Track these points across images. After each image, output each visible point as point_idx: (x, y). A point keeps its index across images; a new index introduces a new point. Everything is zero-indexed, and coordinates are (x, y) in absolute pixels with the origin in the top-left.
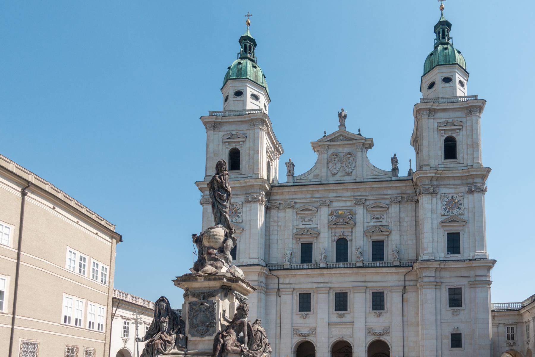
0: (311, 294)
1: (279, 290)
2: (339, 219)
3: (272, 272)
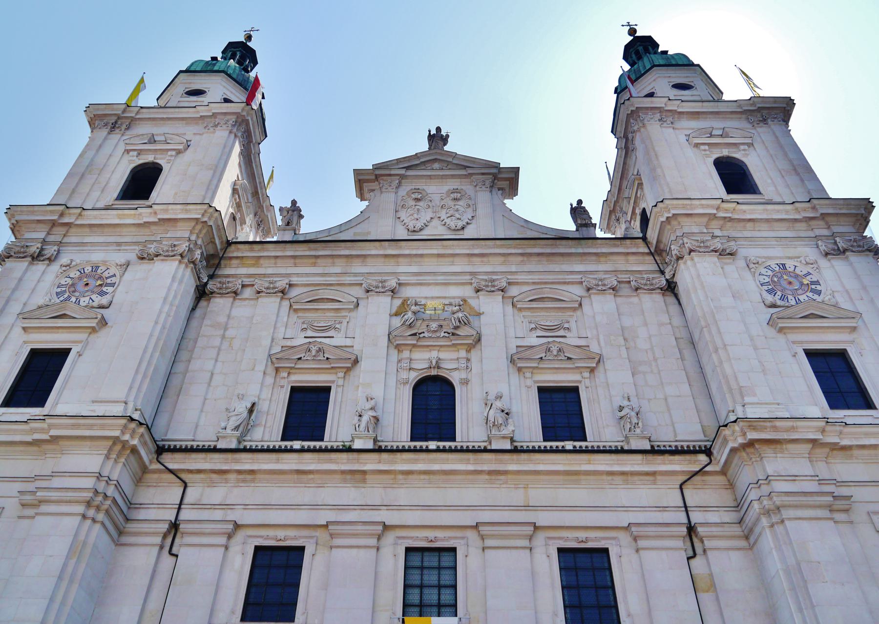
1: (174, 526)
2: (426, 323)
3: (167, 458)
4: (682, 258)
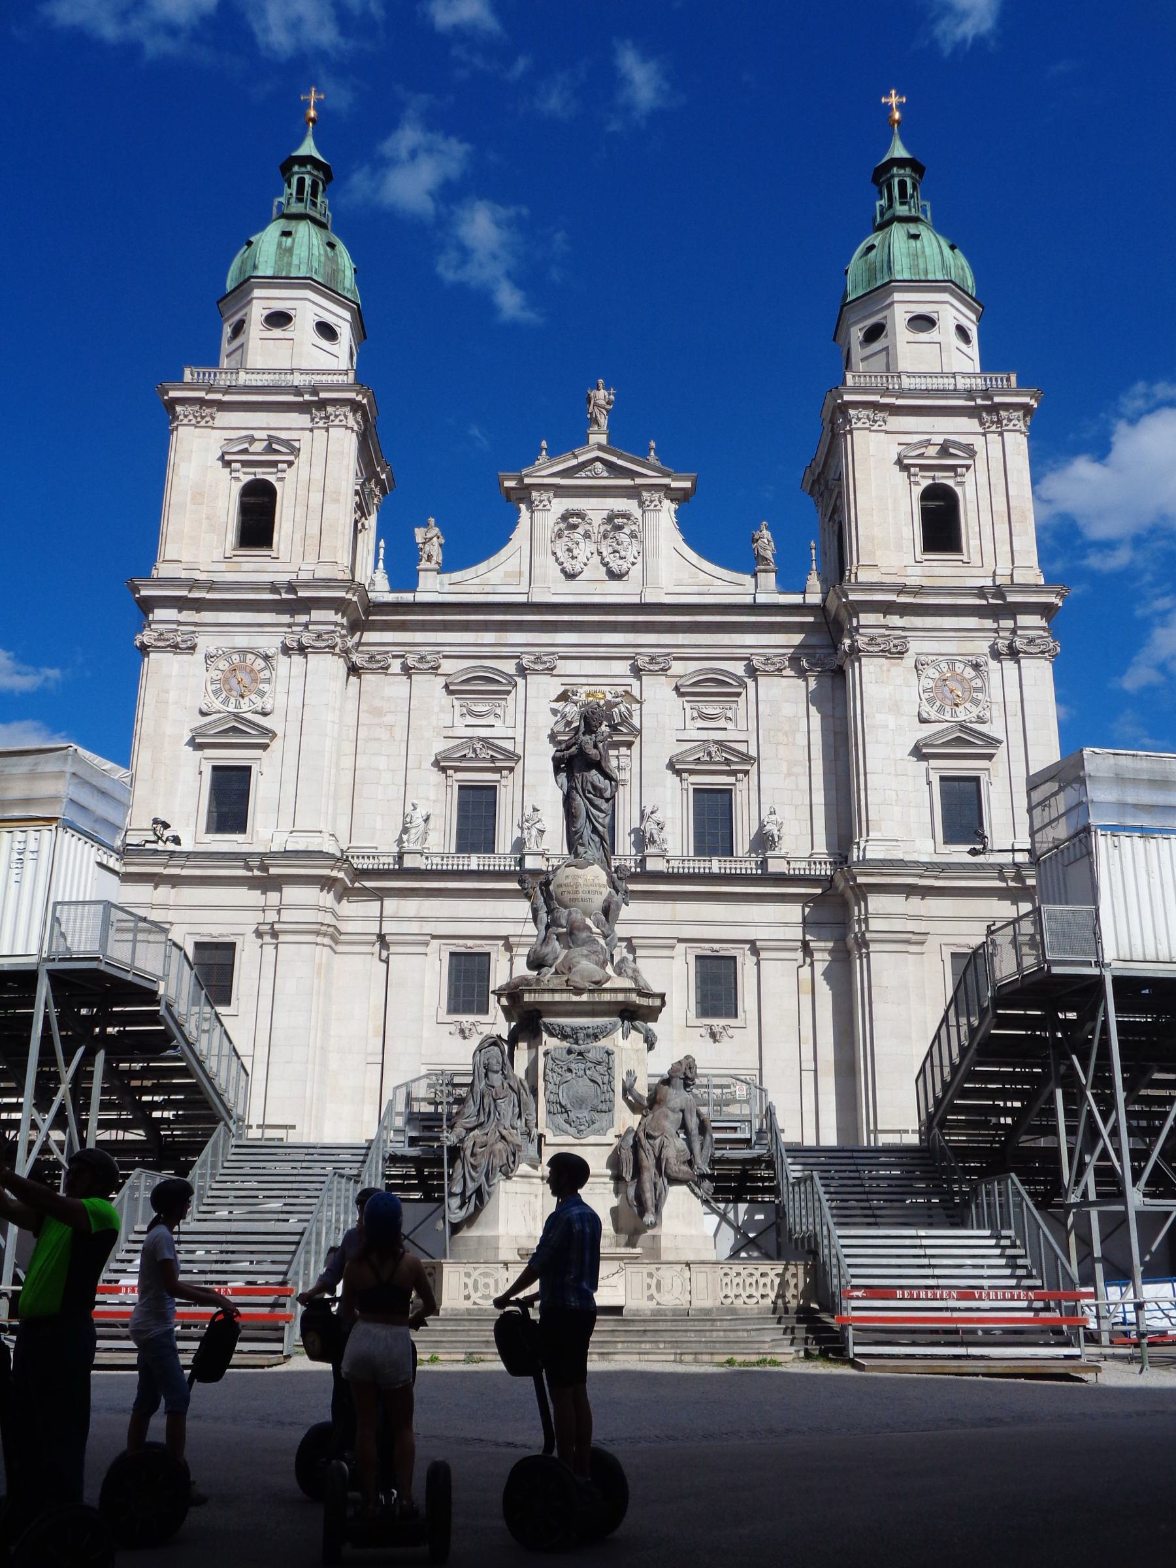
0: (489, 954)
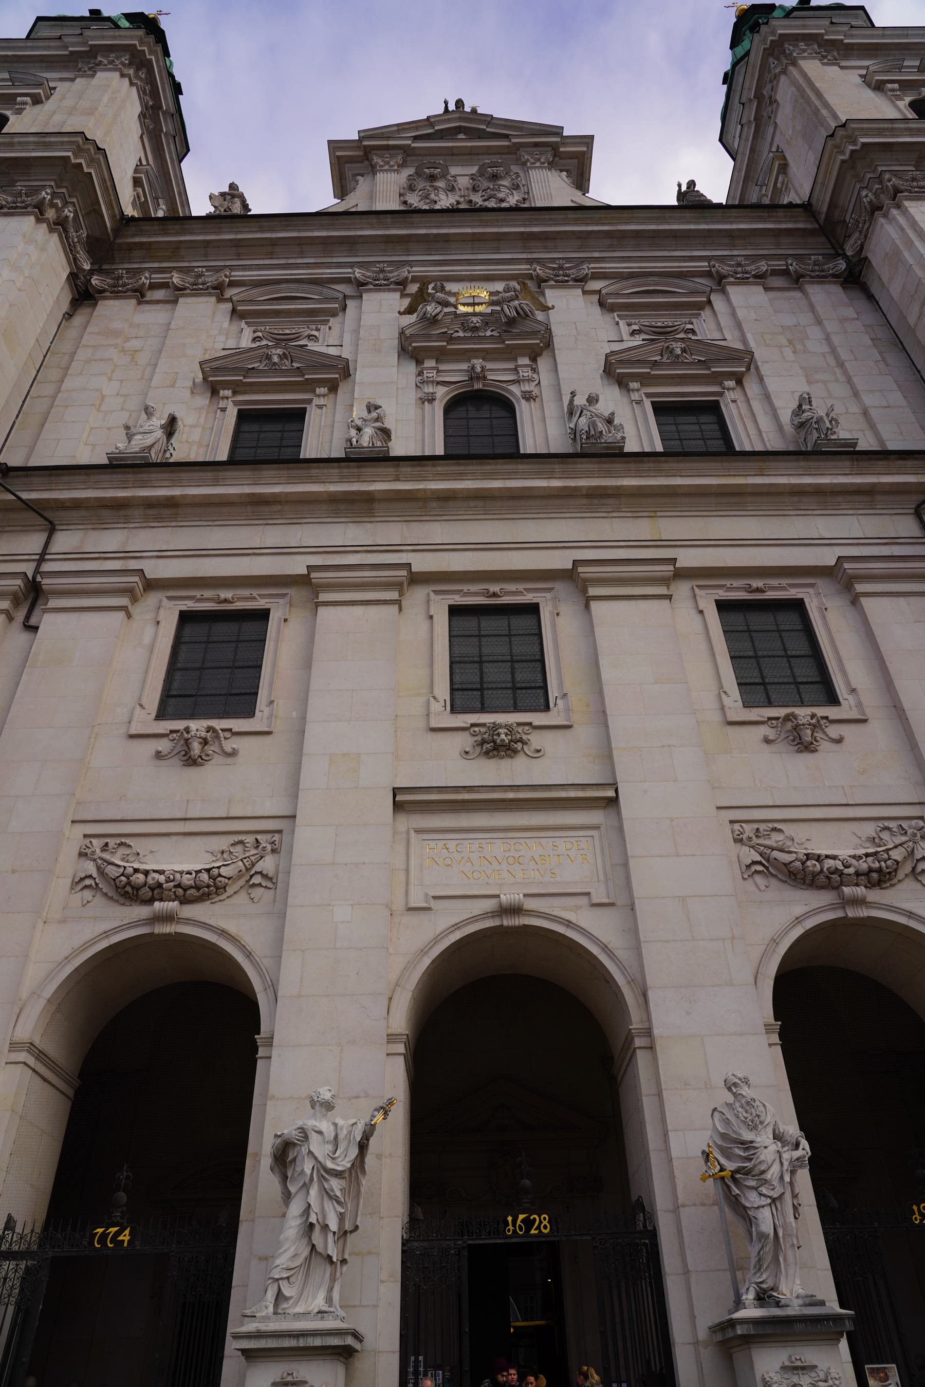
4: (880, 208)
